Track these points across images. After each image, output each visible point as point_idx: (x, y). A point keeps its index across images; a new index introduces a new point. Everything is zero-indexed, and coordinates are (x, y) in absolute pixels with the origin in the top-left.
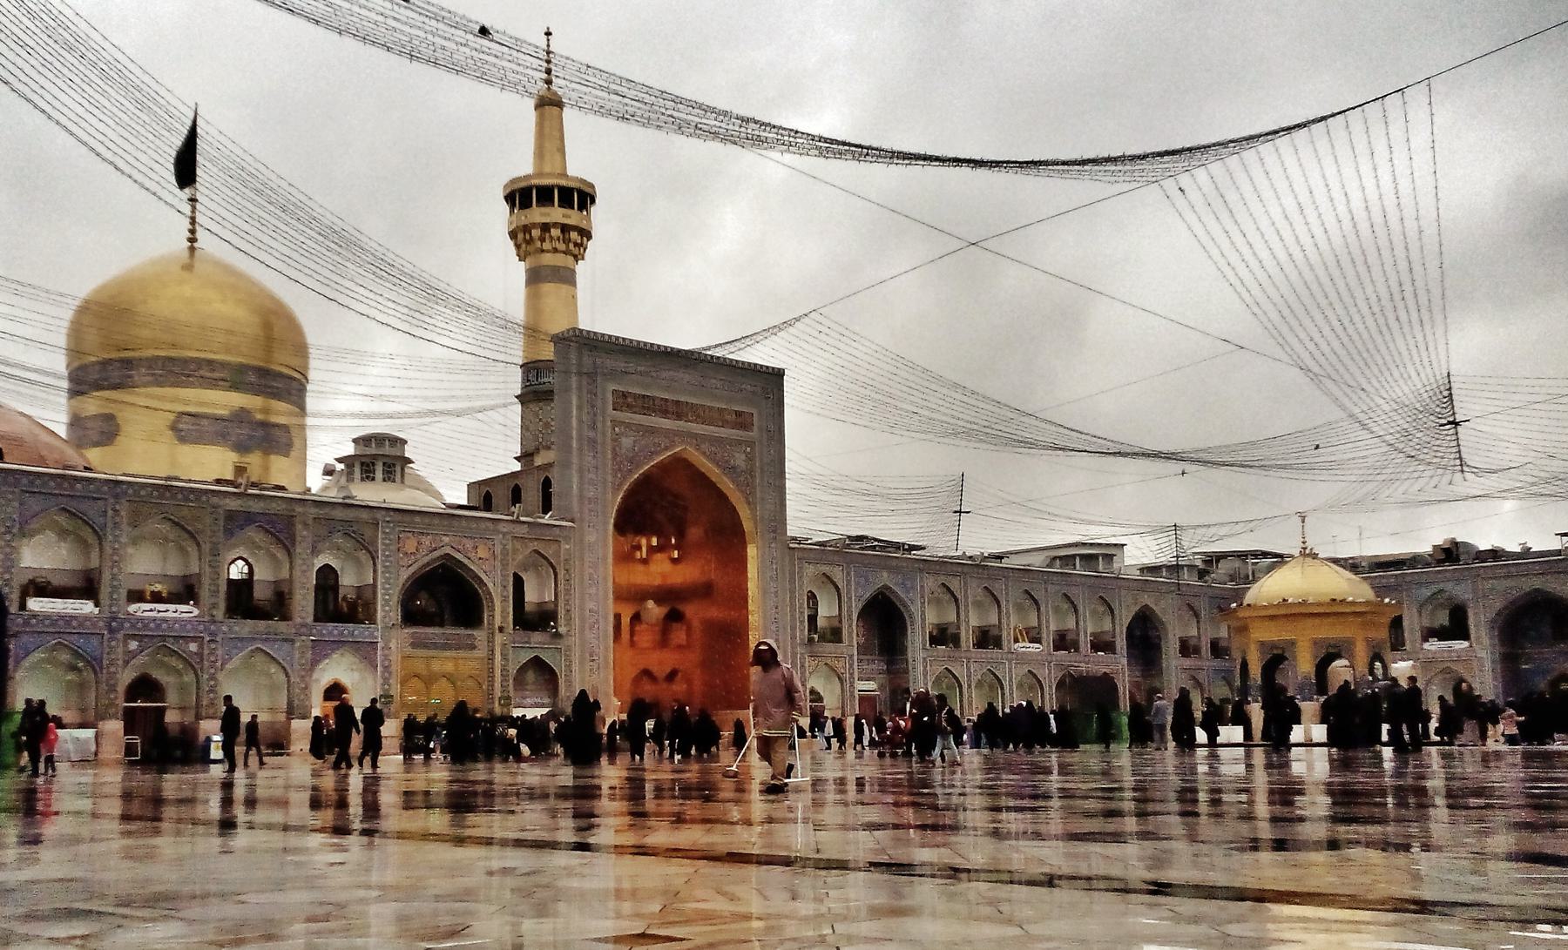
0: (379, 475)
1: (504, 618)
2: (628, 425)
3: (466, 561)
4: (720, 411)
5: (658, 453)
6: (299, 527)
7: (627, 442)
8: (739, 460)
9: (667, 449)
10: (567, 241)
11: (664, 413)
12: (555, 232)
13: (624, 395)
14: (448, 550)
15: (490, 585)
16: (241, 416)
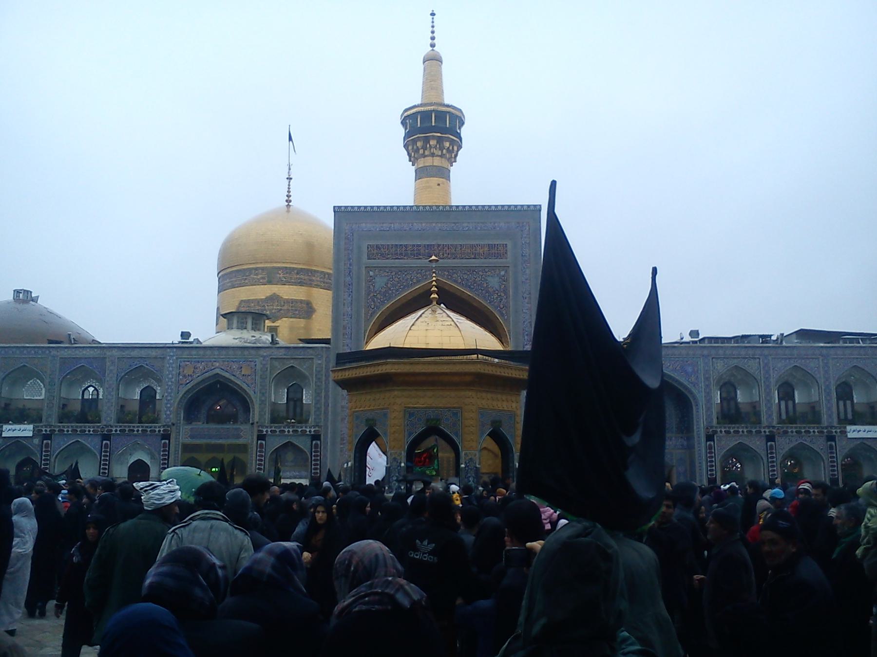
0: (249, 325)
1: (261, 415)
2: (381, 268)
3: (232, 378)
4: (472, 246)
5: (408, 286)
6: (108, 364)
7: (380, 282)
8: (494, 282)
9: (418, 282)
10: (441, 149)
11: (417, 255)
12: (433, 142)
13: (378, 247)
14: (218, 371)
15: (251, 393)
16: (274, 298)
